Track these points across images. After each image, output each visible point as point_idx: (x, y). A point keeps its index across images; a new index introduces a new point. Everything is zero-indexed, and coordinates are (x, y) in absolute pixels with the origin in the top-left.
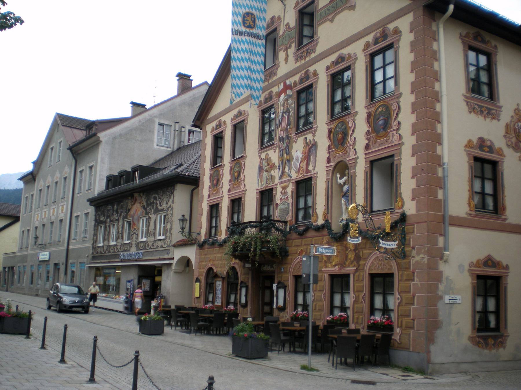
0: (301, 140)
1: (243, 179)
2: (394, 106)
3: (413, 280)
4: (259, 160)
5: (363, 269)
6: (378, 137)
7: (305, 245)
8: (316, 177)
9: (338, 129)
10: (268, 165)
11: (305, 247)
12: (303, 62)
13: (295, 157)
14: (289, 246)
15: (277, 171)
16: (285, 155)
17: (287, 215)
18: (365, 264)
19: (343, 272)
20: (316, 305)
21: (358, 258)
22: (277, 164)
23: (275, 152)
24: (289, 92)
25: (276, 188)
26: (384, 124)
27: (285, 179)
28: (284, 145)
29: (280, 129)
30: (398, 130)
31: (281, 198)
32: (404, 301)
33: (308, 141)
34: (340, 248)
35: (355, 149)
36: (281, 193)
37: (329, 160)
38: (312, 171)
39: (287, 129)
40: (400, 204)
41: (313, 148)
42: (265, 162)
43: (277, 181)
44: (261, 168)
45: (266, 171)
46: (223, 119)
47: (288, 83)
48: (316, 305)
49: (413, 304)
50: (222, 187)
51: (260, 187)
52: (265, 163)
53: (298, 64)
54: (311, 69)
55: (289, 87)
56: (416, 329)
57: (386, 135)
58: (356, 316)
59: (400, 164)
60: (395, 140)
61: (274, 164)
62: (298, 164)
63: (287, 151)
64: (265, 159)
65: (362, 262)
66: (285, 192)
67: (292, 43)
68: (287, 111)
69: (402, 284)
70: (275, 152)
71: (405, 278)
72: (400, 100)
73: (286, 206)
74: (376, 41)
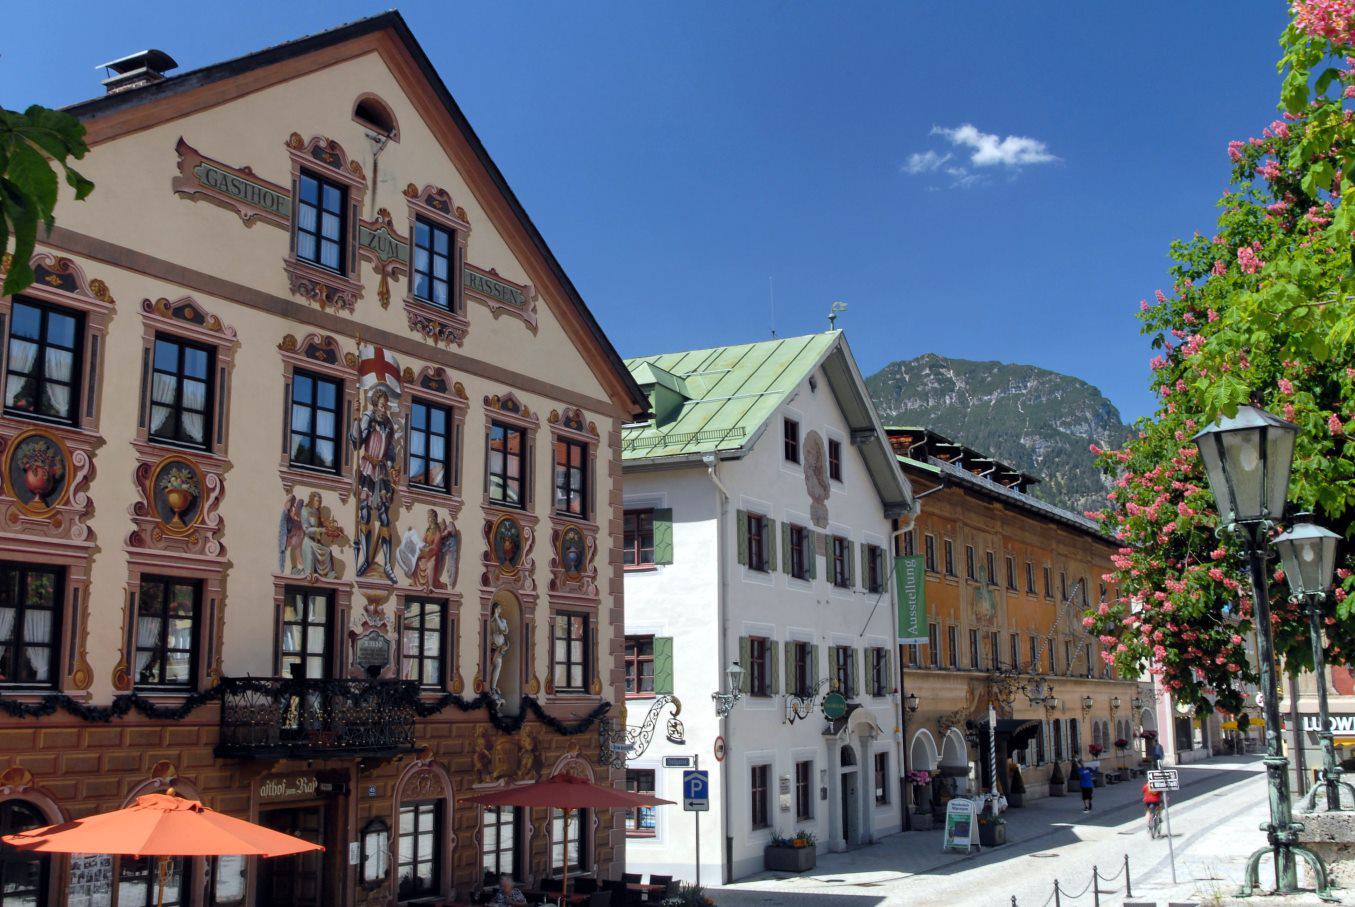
0: (421, 511)
4: (285, 498)
7: (432, 737)
11: (434, 742)
13: (404, 542)
16: (377, 524)
20: (460, 858)
22: (350, 531)
23: (344, 501)
24: (390, 379)
25: (350, 594)
27: (374, 578)
28: (375, 500)
29: (362, 452)
30: (594, 578)
32: (602, 825)
33: (440, 520)
34: (507, 746)
36: (366, 610)
38: (449, 587)
39: (383, 467)
41: (451, 541)
42: (311, 514)
43: (350, 575)
44: (291, 524)
45: (313, 539)
47: (389, 356)
48: (460, 858)
49: (612, 827)
51: (288, 572)
53: (417, 336)
54: (454, 376)
55: (394, 371)
57: (579, 579)
58: (535, 861)
62: (414, 561)
63: (384, 516)
64: (310, 504)
67: (403, 272)
68: (386, 423)
70: (344, 501)
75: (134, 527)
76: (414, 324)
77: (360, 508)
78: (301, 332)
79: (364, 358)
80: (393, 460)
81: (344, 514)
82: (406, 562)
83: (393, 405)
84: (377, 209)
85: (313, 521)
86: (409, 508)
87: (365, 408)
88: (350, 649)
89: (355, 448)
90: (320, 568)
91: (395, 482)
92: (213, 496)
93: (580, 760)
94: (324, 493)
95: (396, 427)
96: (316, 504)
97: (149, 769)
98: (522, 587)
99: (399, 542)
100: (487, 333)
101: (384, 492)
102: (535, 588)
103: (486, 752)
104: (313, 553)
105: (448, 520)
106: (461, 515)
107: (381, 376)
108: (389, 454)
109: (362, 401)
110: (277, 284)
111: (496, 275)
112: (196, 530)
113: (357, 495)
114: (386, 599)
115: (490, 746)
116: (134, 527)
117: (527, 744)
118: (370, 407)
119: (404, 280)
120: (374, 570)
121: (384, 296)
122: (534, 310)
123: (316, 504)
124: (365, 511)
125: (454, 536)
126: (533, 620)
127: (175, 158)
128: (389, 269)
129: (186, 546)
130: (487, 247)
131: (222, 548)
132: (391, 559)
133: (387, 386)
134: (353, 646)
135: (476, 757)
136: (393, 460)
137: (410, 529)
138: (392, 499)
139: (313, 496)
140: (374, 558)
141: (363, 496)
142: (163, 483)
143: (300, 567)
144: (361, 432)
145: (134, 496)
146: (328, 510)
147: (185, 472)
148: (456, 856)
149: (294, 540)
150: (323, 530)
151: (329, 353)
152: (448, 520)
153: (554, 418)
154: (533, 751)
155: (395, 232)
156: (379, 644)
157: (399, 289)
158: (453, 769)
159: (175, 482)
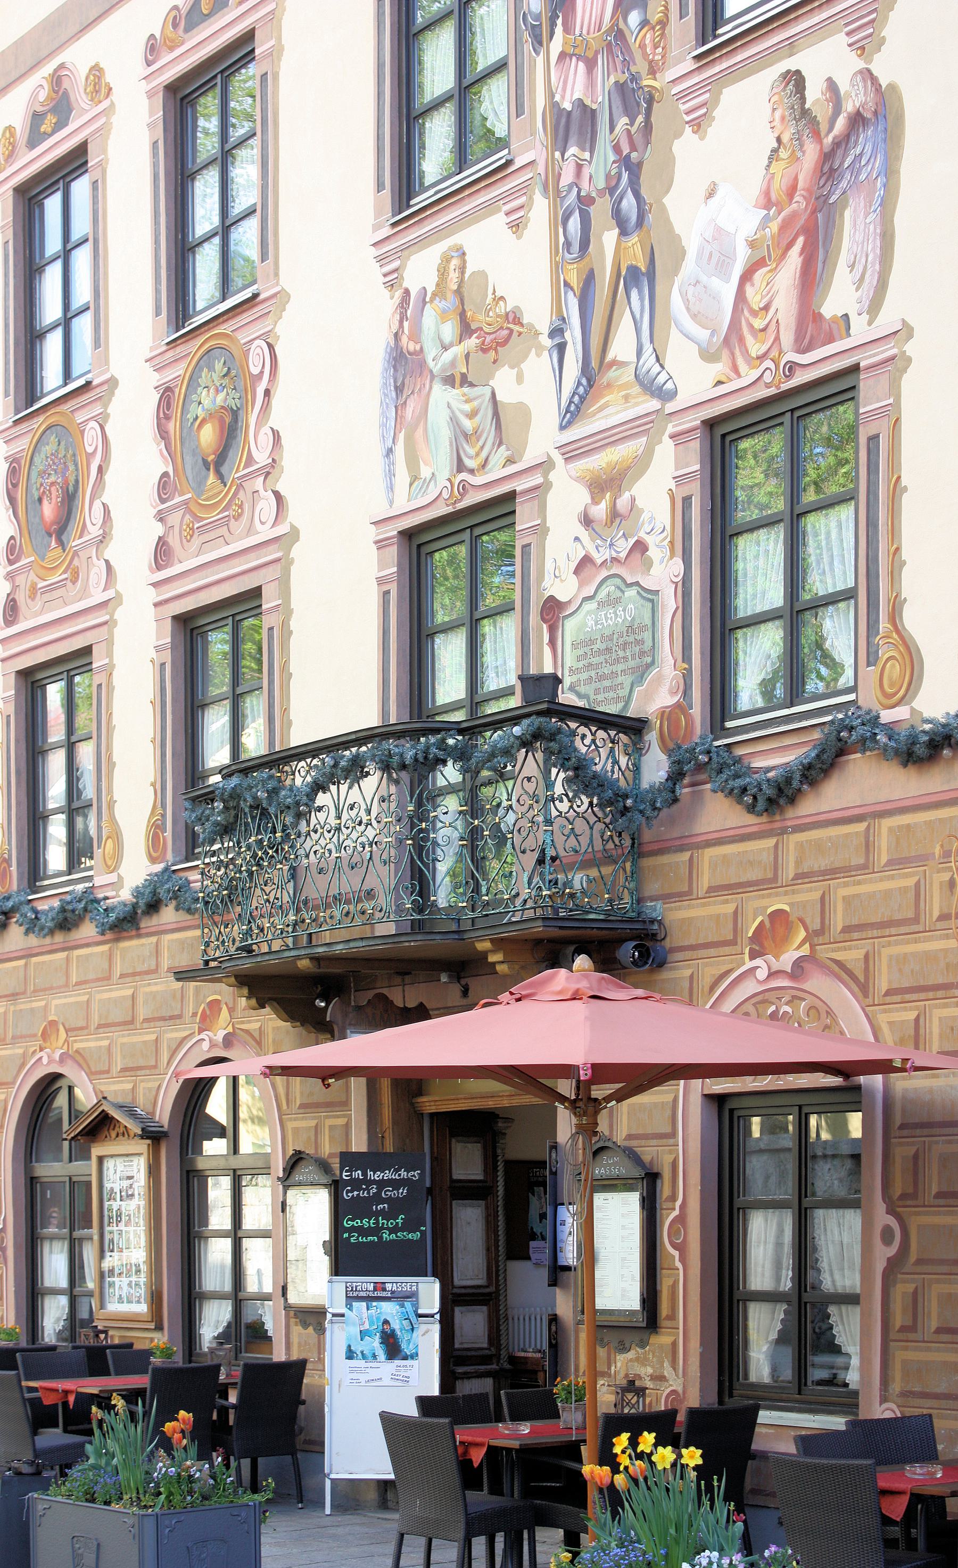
0: (748, 107)
1: (262, 458)
4: (388, 303)
8: (896, 365)
10: (466, 329)
11: (810, 894)
13: (692, 245)
14: (666, 897)
15: (539, 365)
17: (641, 672)
22: (539, 316)
25: (539, 491)
27: (610, 412)
29: (556, 45)
31: (586, 561)
33: (814, 93)
36: (587, 521)
38: (859, 325)
41: (865, 142)
42: (443, 316)
43: (543, 437)
45: (449, 381)
46: (78, 58)
50: (103, 539)
52: (437, 327)
61: (515, 318)
63: (629, 203)
64: (440, 291)
66: (614, 515)
70: (516, 227)
73: (632, 607)
86: (698, 126)
88: (547, 651)
97: (195, 1014)
104: (454, 420)
114: (641, 464)
124: (574, 223)
134: (552, 643)
137: (711, 194)
141: (567, 178)
143: (425, 472)
158: (882, 983)
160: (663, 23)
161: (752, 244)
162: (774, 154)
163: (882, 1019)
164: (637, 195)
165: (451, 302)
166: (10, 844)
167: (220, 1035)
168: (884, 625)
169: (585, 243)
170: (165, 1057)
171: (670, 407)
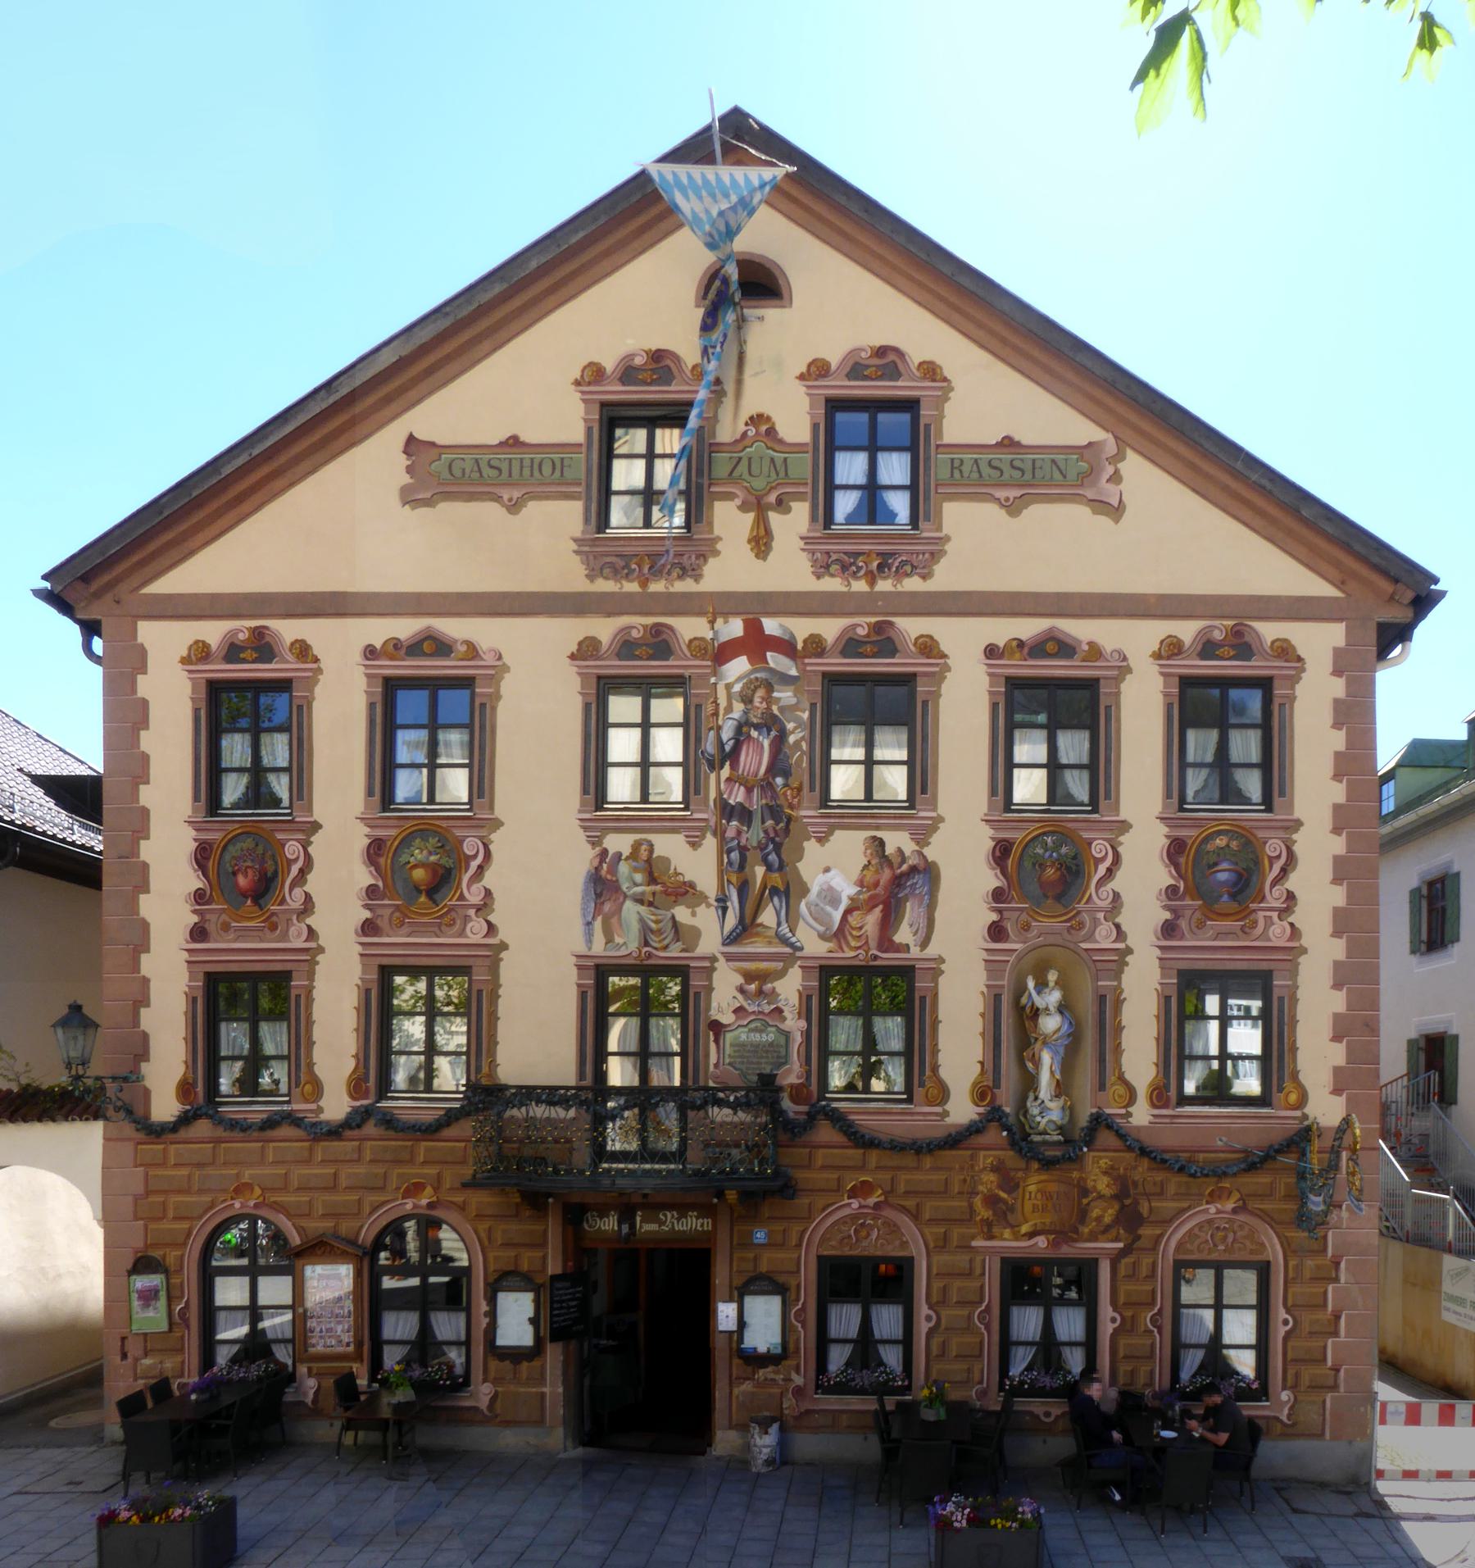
2: (1273, 847)
3: (1336, 1280)
5: (1154, 1248)
6: (1211, 911)
9: (1039, 851)
12: (860, 586)
13: (815, 889)
14: (794, 1167)
16: (760, 871)
18: (1161, 1236)
19: (1066, 1251)
20: (944, 1345)
21: (1130, 1219)
24: (774, 660)
25: (712, 969)
26: (1236, 884)
28: (754, 835)
29: (726, 772)
33: (890, 850)
34: (1053, 1188)
35: (1118, 926)
36: (741, 990)
37: (996, 932)
39: (767, 786)
40: (1293, 1098)
41: (918, 879)
43: (710, 942)
44: (602, 887)
47: (771, 626)
49: (1336, 1334)
51: (599, 947)
53: (832, 584)
54: (911, 627)
55: (786, 646)
56: (1342, 1389)
57: (1244, 913)
59: (1294, 1000)
60: (1278, 934)
62: (837, 916)
63: (773, 857)
65: (1146, 1231)
66: (760, 992)
67: (799, 497)
68: (770, 723)
69: (1294, 1289)
70: (694, 845)
71: (1307, 1274)
72: (1295, 837)
74: (1208, 648)
75: (367, 914)
76: (822, 568)
77: (724, 849)
78: (604, 629)
79: (723, 638)
80: (786, 774)
81: (699, 864)
82: (820, 917)
83: (785, 695)
84: (744, 416)
85: (639, 877)
87: (729, 709)
88: (713, 1046)
89: (712, 767)
90: (654, 940)
91: (791, 807)
92: (474, 864)
93: (1241, 1217)
94: (654, 838)
95: (790, 726)
96: (644, 854)
98: (1090, 937)
99: (805, 891)
100: (982, 544)
101: (770, 823)
102: (1121, 934)
103: (1003, 1195)
104: (642, 920)
105: (909, 847)
106: (935, 839)
107: (757, 657)
108: (779, 765)
109: (723, 702)
110: (572, 576)
111: (1018, 444)
112: (451, 909)
113: (719, 833)
114: (781, 974)
115: (1010, 1184)
116: (367, 914)
117: (1103, 1185)
118: (738, 708)
119: (801, 512)
120: (758, 934)
121: (761, 543)
122: (1116, 478)
123: (644, 854)
124: (735, 855)
125: (928, 872)
126: (1118, 990)
127: (403, 461)
128: (772, 498)
129: (439, 928)
130: (990, 399)
131: (491, 929)
132: (791, 917)
133: (772, 670)
134: (717, 1041)
135: (978, 1202)
136: (786, 774)
137: (827, 870)
138: (787, 830)
139: (636, 846)
140: (756, 914)
142: (403, 859)
143: (618, 940)
144: (720, 744)
145: (364, 877)
146: (666, 861)
147: (433, 841)
148: (936, 1341)
149: (607, 907)
150: (658, 888)
151: (659, 643)
152: (909, 847)
153: (1171, 649)
154: (1115, 1197)
155: (781, 442)
156: (770, 1036)
157: (793, 524)
159: (419, 855)
160: (800, 789)
161: (851, 899)
162: (865, 867)
163: (926, 1231)
164: (779, 856)
165: (641, 864)
166: (195, 1072)
167: (424, 1202)
168: (928, 1072)
169: (742, 867)
170: (367, 1209)
171: (798, 954)
